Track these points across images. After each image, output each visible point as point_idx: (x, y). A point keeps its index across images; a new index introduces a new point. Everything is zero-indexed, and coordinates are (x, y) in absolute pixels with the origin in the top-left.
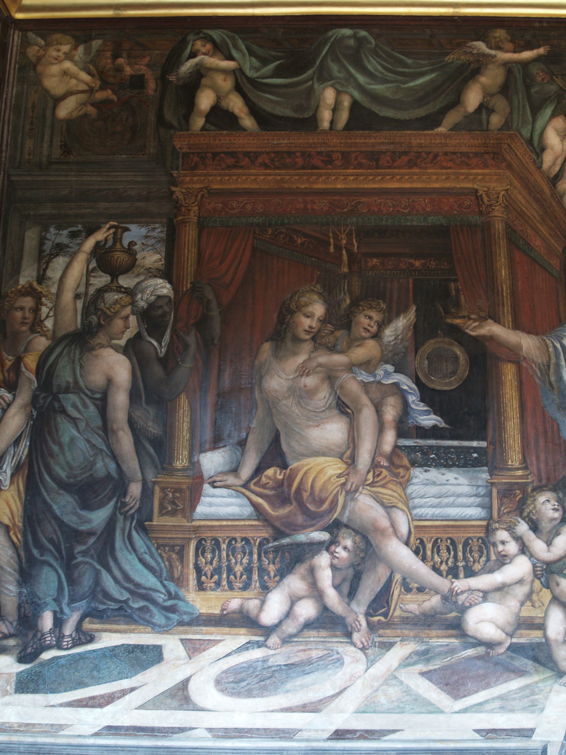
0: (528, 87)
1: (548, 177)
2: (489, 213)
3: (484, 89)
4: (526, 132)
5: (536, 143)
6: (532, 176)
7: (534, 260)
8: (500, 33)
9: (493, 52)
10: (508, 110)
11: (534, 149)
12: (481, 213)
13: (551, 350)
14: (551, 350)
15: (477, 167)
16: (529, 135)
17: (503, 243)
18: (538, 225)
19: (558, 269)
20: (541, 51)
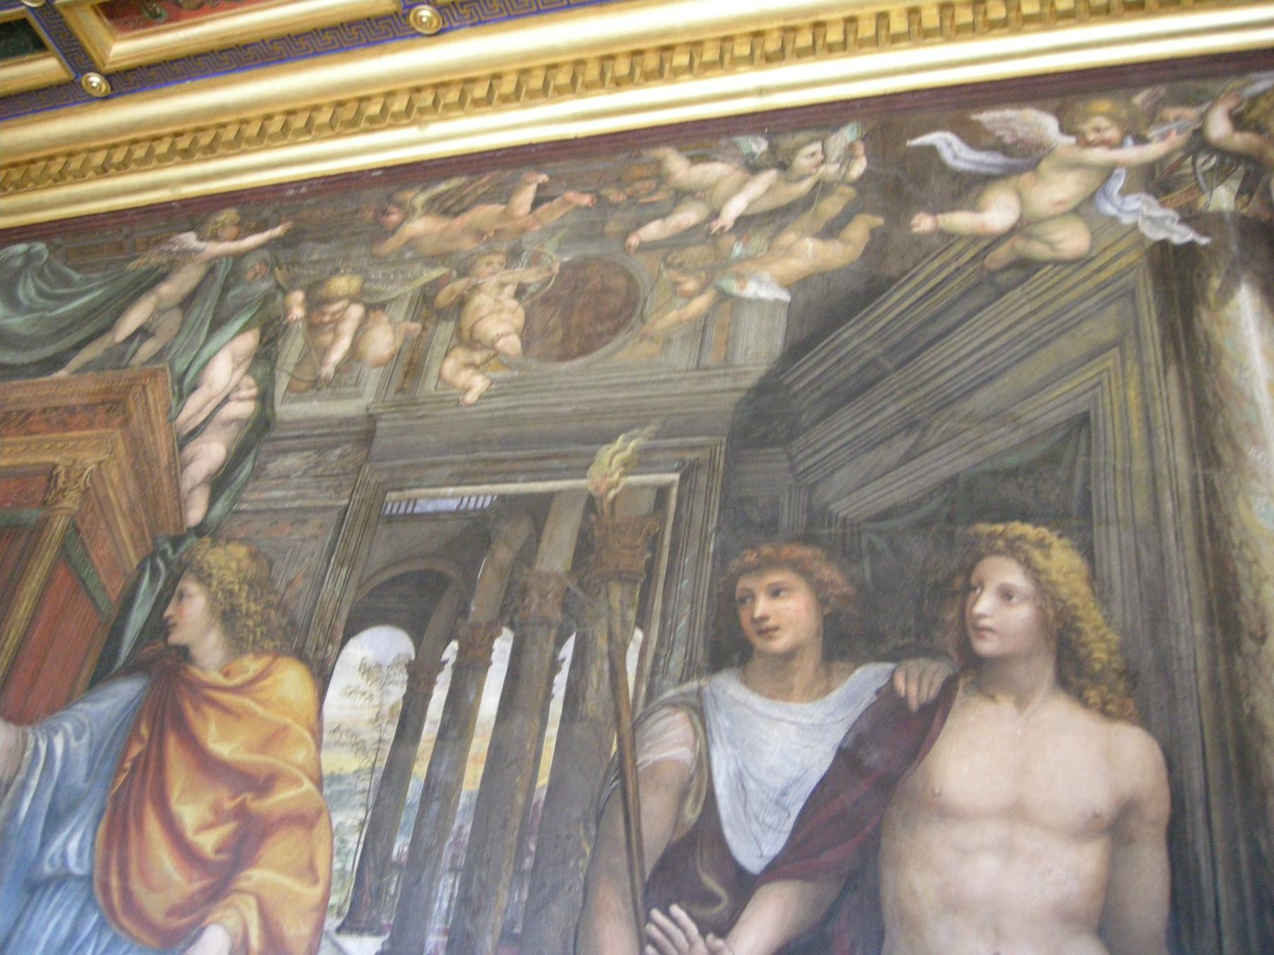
0: (225, 289)
1: (178, 435)
2: (56, 502)
3: (160, 300)
4: (180, 366)
5: (188, 380)
6: (153, 432)
7: (84, 582)
8: (229, 215)
9: (201, 245)
10: (175, 331)
11: (181, 389)
12: (45, 503)
13: (28, 754)
14: (28, 754)
15: (79, 427)
16: (185, 367)
17: (48, 555)
18: (119, 519)
19: (114, 598)
20: (278, 231)
